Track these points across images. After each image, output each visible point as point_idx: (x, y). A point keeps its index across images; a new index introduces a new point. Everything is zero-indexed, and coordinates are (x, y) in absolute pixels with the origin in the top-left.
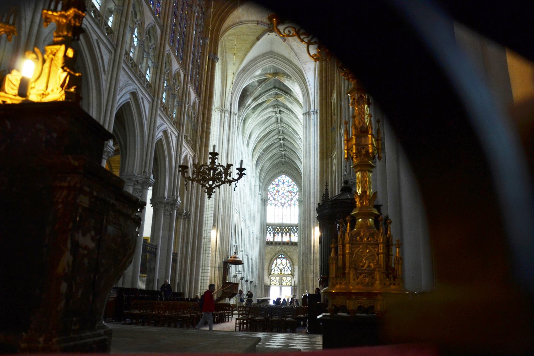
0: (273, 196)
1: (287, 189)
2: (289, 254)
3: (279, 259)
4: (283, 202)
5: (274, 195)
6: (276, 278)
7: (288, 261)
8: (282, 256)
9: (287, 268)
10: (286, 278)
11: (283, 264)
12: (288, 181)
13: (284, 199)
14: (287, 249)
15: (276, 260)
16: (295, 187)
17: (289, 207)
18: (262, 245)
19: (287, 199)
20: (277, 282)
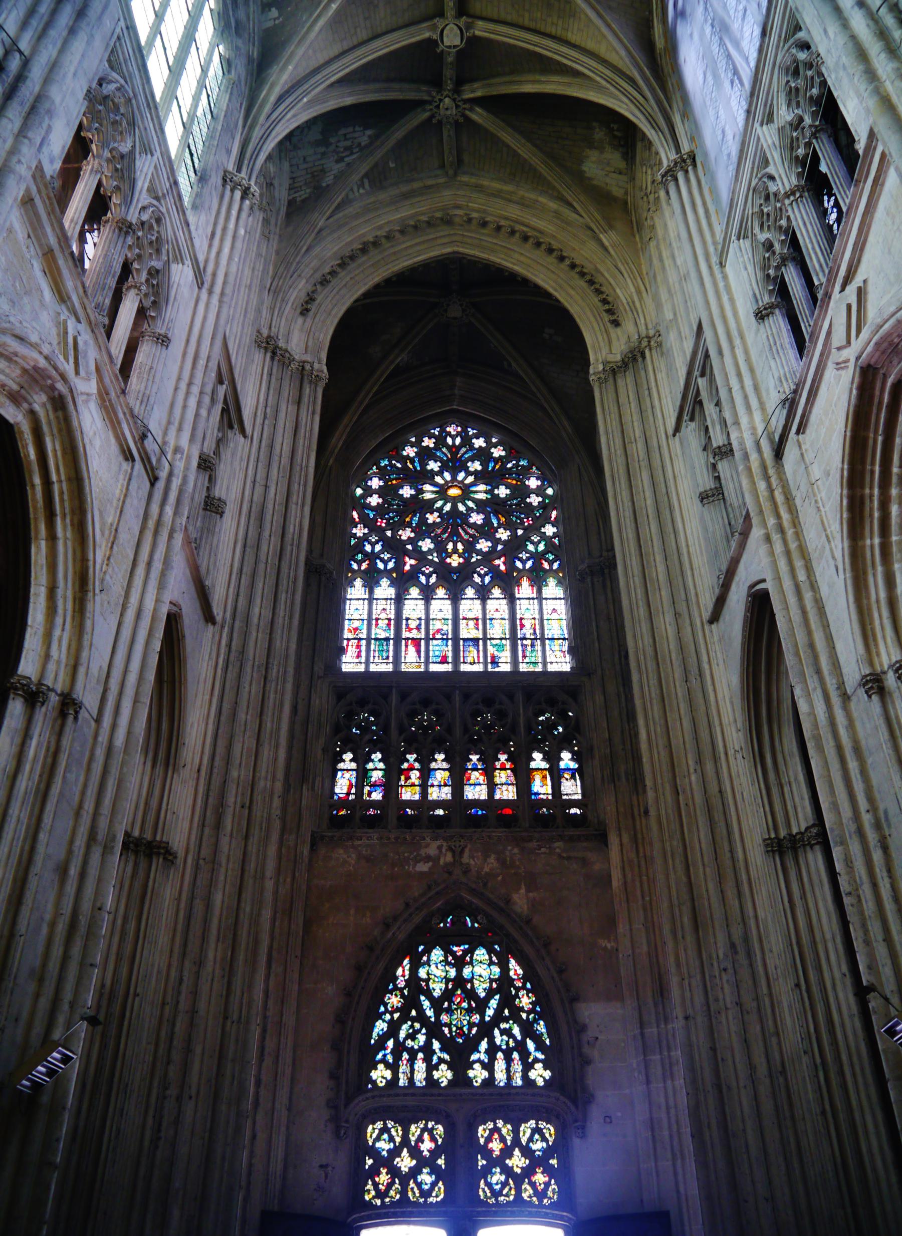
0: (389, 533)
1: (481, 492)
2: (521, 901)
3: (437, 954)
4: (455, 561)
5: (395, 528)
6: (415, 1130)
7: (515, 969)
8: (459, 922)
9: (516, 1031)
10: (506, 1129)
11: (471, 994)
12: (483, 455)
13: (460, 547)
14: (502, 862)
15: (406, 962)
16: (533, 483)
17: (497, 592)
18: (250, 688)
19: (484, 545)
20: (426, 1178)
